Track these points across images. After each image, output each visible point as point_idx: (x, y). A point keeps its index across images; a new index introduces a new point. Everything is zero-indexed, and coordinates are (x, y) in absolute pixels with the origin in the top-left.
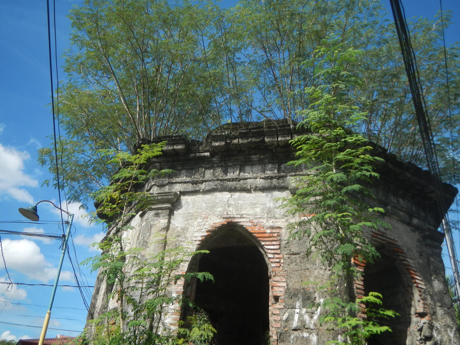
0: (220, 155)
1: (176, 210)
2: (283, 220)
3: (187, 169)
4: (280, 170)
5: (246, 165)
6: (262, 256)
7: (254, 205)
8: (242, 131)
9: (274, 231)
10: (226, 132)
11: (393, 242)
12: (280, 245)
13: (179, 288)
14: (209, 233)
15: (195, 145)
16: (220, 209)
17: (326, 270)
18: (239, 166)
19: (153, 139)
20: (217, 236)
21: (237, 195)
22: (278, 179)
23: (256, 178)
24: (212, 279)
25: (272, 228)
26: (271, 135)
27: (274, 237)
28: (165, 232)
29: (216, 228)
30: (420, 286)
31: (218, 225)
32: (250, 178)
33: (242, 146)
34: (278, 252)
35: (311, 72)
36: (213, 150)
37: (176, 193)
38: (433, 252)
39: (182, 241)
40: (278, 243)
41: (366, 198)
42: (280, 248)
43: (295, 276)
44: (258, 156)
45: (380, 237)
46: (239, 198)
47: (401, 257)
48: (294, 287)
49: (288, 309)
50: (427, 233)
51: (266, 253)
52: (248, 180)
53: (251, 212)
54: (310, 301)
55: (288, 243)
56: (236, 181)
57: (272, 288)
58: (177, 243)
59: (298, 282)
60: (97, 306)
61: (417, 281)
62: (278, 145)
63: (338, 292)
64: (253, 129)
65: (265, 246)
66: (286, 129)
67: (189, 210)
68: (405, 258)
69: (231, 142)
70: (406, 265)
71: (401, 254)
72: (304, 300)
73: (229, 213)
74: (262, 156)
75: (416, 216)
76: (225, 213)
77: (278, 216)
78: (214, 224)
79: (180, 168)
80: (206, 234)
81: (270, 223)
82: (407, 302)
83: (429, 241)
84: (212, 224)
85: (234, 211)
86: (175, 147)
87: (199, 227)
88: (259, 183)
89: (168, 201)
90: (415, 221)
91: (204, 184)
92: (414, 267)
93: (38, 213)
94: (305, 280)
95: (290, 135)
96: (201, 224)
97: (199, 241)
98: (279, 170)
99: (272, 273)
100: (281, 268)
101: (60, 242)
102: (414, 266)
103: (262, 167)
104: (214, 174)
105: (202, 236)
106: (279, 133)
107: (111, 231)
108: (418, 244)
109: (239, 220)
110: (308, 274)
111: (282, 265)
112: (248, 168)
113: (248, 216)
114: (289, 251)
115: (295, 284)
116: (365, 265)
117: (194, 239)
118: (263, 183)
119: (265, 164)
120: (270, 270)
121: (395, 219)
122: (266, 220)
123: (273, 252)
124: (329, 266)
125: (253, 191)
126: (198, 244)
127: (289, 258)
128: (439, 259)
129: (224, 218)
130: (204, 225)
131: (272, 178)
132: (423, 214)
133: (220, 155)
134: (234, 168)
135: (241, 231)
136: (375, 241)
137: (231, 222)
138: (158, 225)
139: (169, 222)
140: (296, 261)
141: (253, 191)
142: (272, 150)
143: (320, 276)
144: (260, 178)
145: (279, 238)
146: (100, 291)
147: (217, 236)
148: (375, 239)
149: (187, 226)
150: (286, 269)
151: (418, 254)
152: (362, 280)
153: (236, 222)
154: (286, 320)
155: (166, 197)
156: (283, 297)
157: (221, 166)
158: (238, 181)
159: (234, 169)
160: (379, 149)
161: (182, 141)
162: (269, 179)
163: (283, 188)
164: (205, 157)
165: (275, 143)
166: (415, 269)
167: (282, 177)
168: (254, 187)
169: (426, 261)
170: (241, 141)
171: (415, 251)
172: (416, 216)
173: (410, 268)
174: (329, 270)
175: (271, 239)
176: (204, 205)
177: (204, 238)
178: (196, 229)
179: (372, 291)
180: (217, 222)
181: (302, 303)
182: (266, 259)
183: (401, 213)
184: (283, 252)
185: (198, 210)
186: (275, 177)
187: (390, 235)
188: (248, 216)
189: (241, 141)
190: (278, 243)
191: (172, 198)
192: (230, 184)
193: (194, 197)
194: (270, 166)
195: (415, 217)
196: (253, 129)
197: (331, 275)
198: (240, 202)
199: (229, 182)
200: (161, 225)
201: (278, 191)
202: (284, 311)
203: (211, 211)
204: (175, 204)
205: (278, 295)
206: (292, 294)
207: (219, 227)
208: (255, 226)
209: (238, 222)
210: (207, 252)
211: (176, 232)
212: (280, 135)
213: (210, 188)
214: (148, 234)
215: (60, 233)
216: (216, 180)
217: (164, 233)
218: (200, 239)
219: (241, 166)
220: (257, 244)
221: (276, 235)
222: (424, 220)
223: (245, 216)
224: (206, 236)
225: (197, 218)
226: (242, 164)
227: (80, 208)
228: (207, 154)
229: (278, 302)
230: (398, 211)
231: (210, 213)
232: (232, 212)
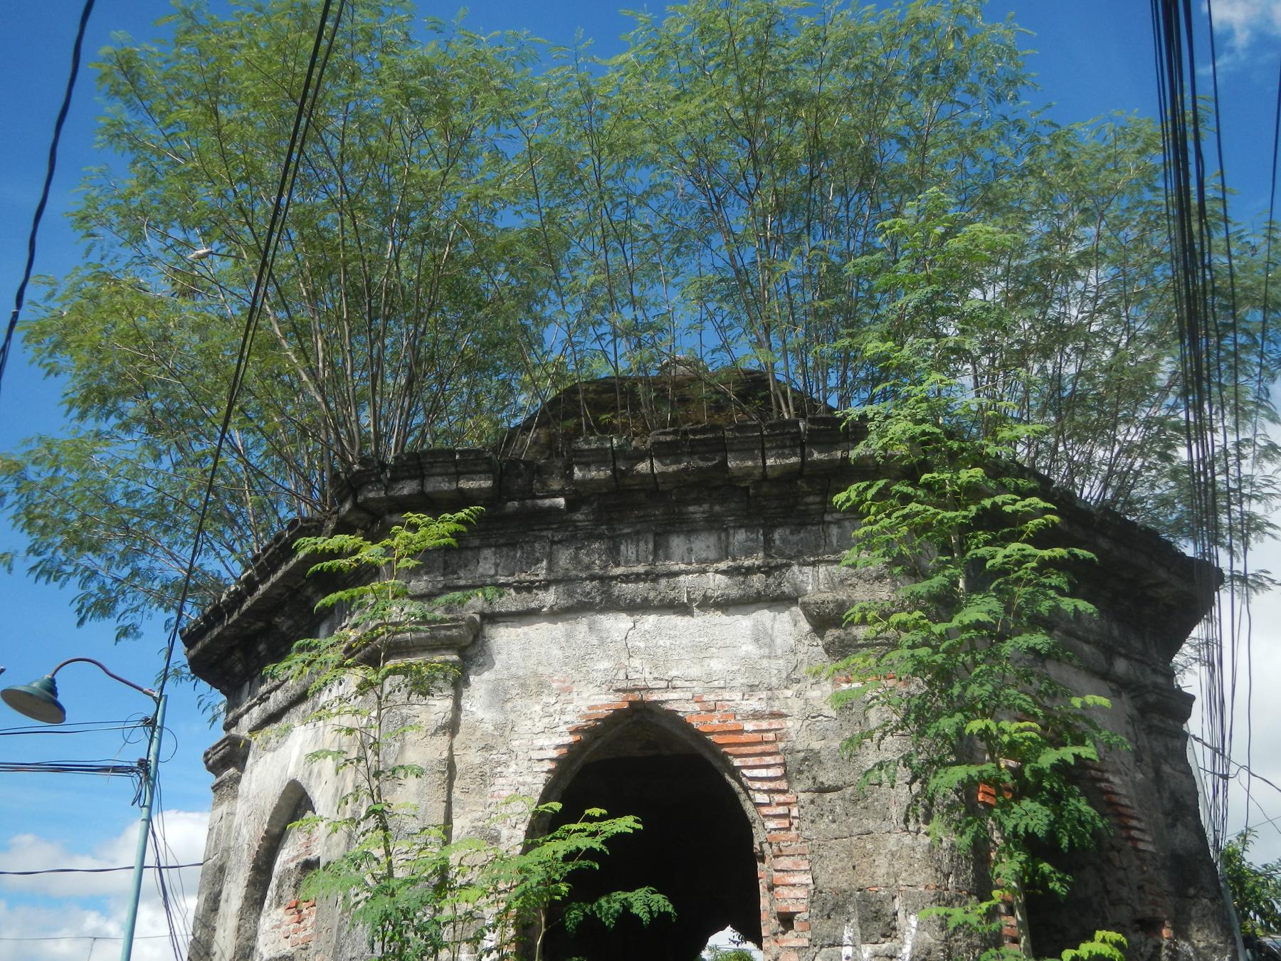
0: (595, 505)
1: (474, 668)
2: (789, 693)
3: (498, 546)
4: (771, 548)
5: (671, 532)
6: (735, 796)
7: (702, 650)
8: (662, 438)
9: (764, 725)
10: (615, 441)
12: (784, 764)
14: (578, 738)
15: (519, 475)
16: (605, 664)
17: (918, 832)
18: (651, 538)
19: (396, 458)
20: (599, 742)
21: (650, 621)
22: (768, 574)
23: (704, 571)
24: (670, 909)
25: (757, 716)
26: (745, 450)
27: (767, 742)
28: (447, 738)
29: (597, 720)
30: (1141, 846)
31: (603, 713)
32: (687, 573)
33: (659, 480)
34: (783, 785)
35: (1045, 467)
36: (576, 492)
37: (472, 620)
38: (1166, 747)
39: (499, 764)
40: (778, 759)
42: (786, 776)
43: (833, 853)
44: (706, 507)
46: (659, 631)
47: (1093, 772)
48: (834, 885)
49: (822, 947)
50: (1151, 698)
51: (746, 789)
52: (682, 578)
53: (695, 671)
54: (881, 924)
55: (805, 759)
56: (645, 581)
57: (771, 888)
58: (487, 768)
59: (844, 869)
60: (215, 948)
61: (1134, 833)
62: (764, 477)
63: (953, 892)
64: (694, 432)
65: (744, 771)
66: (788, 433)
67: (513, 670)
68: (1102, 771)
69: (631, 469)
70: (1108, 792)
72: (863, 922)
73: (633, 675)
74: (717, 508)
75: (1123, 651)
76: (621, 676)
77: (774, 681)
78: (590, 708)
79: (477, 542)
80: (570, 739)
81: (754, 704)
82: (1108, 892)
83: (1156, 720)
84: (584, 708)
85: (647, 670)
86: (465, 484)
87: (546, 720)
88: (712, 585)
89: (449, 645)
90: (1121, 666)
91: (552, 589)
92: (1126, 796)
93: (60, 699)
94: (864, 866)
95: (798, 451)
96: (552, 710)
97: (552, 760)
98: (768, 545)
99: (766, 846)
100: (793, 832)
101: (128, 784)
102: (1123, 792)
103: (719, 538)
104: (575, 559)
105: (558, 747)
106: (768, 445)
107: (241, 715)
108: (1130, 729)
109: (664, 697)
110: (869, 846)
111: (796, 822)
112: (677, 544)
113: (688, 684)
114: (810, 782)
115: (836, 877)
117: (536, 755)
118: (723, 586)
119: (726, 530)
120: (759, 836)
122: (740, 695)
123: (766, 786)
124: (926, 823)
125: (696, 610)
126: (549, 771)
127: (812, 802)
128: (1182, 767)
129: (618, 690)
130: (563, 712)
131: (750, 571)
132: (1137, 644)
133: (595, 505)
134: (638, 541)
135: (668, 726)
137: (642, 702)
138: (423, 717)
139: (457, 707)
140: (832, 811)
141: (696, 610)
142: (747, 488)
143: (905, 852)
144: (717, 572)
145: (781, 745)
146: (222, 903)
147: (599, 742)
149: (512, 717)
150: (807, 833)
151: (1132, 759)
153: (655, 702)
155: (443, 632)
156: (806, 915)
157: (599, 537)
158: (653, 580)
159: (637, 546)
161: (485, 467)
162: (740, 574)
163: (780, 601)
164: (554, 510)
165: (756, 472)
167: (778, 567)
168: (700, 598)
169: (1151, 775)
170: (658, 467)
172: (1123, 651)
173: (1115, 799)
174: (927, 834)
175: (759, 749)
176: (556, 652)
177: (564, 750)
178: (540, 726)
179: (1101, 929)
180: (599, 703)
181: (858, 930)
182: (748, 806)
183: (1086, 648)
184: (795, 784)
185: (541, 669)
186: (759, 568)
188: (688, 684)
189: (658, 467)
190: (778, 759)
191: (461, 635)
192: (628, 589)
193: (526, 629)
194: (740, 536)
195: (1121, 655)
196: (694, 432)
197: (931, 847)
198: (661, 643)
199: (626, 582)
200: (433, 717)
201: (769, 608)
202: (810, 954)
203: (577, 669)
204: (470, 652)
205: (792, 909)
206: (830, 906)
207: (607, 717)
208: (711, 711)
209: (662, 702)
210: (626, 824)
211: (478, 734)
212: (772, 448)
213: (570, 602)
214: (398, 744)
215: (132, 756)
216: (586, 579)
217: (442, 741)
218: (555, 754)
219: (656, 534)
220: (717, 764)
221: (771, 736)
222: (1142, 662)
223: (678, 683)
224: (570, 746)
225: (539, 694)
226: (659, 530)
227: (117, 639)
228: (561, 501)
229: (792, 928)
230: (1078, 642)
231: (577, 676)
232: (642, 672)
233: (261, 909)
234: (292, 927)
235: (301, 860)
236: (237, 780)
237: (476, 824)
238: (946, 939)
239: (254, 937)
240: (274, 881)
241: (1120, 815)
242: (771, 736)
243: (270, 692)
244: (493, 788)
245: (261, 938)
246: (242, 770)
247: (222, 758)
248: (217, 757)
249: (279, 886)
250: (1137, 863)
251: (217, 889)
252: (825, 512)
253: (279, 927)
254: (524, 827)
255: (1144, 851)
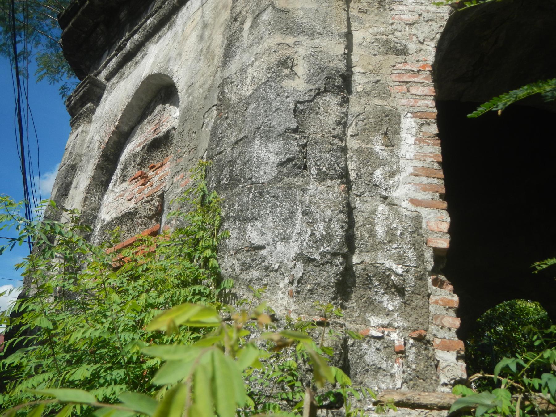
13: (420, 103)
233: (105, 190)
234: (136, 190)
235: (148, 142)
236: (93, 112)
237: (378, 37)
239: (98, 209)
240: (120, 167)
243: (127, 40)
244: (392, 12)
245: (103, 210)
246: (97, 106)
247: (82, 97)
248: (78, 97)
249: (125, 168)
251: (68, 180)
253: (123, 195)
254: (433, 44)
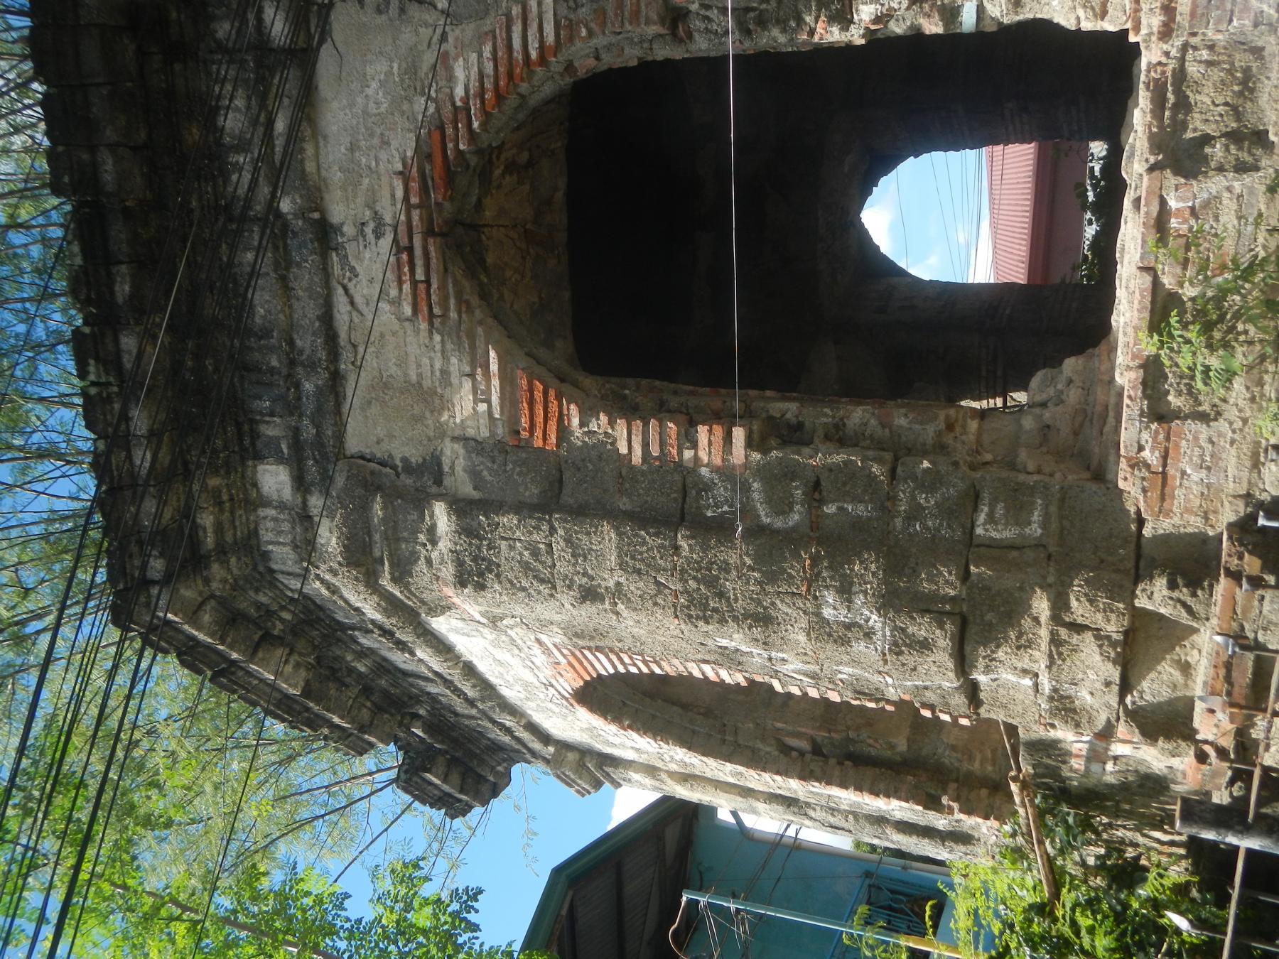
11: (414, 185)
17: (617, 614)
41: (299, 343)
45: (420, 275)
47: (462, 147)
61: (534, 55)
66: (230, 680)
71: (450, 145)
74: (349, 658)
92: (480, 55)
116: (552, 393)
121: (317, 155)
124: (602, 601)
136: (446, 309)
148: (437, 311)
152: (612, 423)
154: (812, 678)
160: (92, 377)
166: (487, 52)
171: (407, 36)
187: (393, 196)
221: (565, 652)
224: (637, 731)
238: (735, 619)
241: (510, 75)
242: (565, 652)
250: (578, 44)
252: (292, 599)
255: (557, 35)
